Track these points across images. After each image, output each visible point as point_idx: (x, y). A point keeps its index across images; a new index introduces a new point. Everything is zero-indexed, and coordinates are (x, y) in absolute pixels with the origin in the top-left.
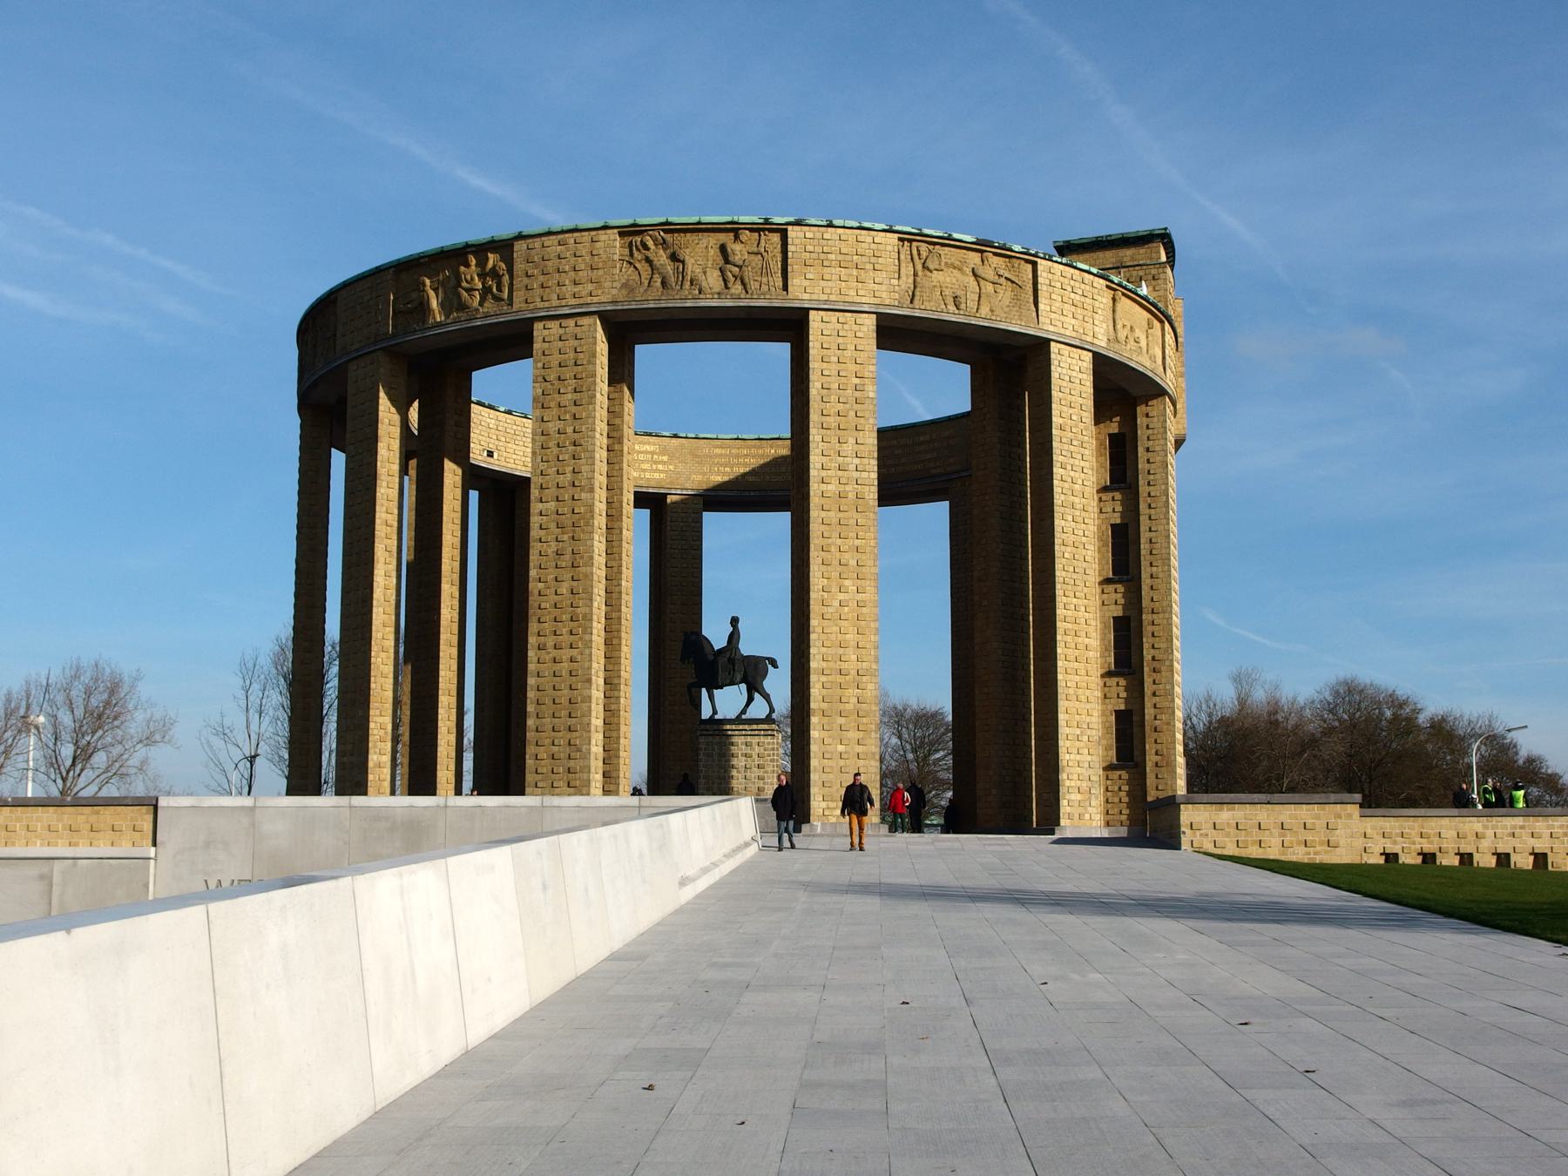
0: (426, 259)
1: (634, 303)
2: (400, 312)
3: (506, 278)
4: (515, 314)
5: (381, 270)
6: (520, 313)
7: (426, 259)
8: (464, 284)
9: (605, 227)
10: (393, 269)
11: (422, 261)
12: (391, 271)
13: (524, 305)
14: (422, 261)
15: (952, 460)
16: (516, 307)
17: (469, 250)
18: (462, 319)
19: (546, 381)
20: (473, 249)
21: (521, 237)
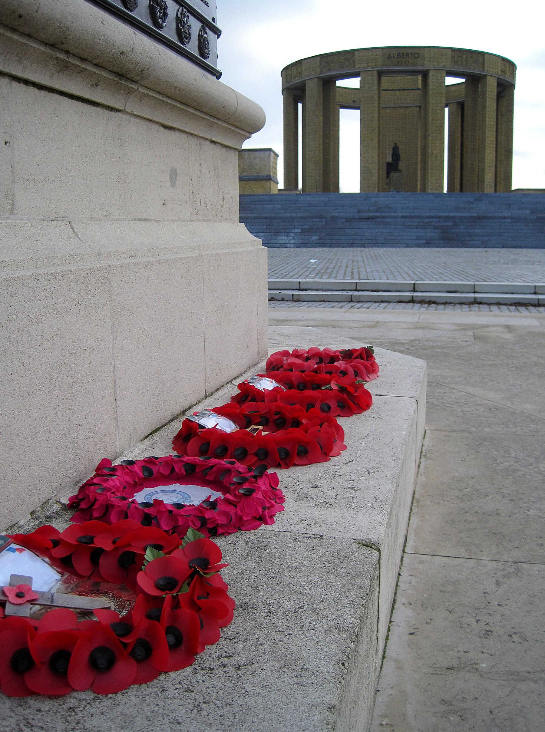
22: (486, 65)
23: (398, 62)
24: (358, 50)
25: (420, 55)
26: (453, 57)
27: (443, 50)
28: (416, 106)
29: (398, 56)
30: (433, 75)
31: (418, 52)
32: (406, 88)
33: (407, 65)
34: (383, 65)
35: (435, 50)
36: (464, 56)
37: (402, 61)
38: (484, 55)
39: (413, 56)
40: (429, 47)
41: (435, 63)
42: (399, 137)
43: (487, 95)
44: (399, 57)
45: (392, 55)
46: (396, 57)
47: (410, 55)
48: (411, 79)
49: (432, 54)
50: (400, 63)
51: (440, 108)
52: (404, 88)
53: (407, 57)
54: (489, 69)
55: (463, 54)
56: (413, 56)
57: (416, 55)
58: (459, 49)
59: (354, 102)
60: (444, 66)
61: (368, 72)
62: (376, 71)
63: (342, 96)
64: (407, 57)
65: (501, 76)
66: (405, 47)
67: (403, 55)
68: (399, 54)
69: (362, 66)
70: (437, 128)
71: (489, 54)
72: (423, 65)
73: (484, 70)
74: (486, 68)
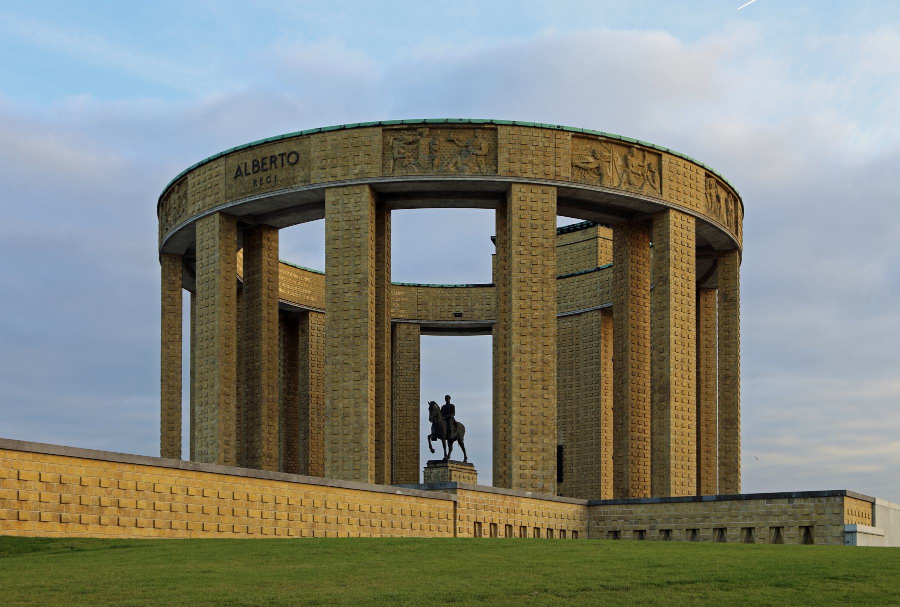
0: (604, 139)
1: (710, 219)
2: (577, 166)
3: (657, 175)
4: (663, 201)
5: (562, 130)
6: (665, 202)
7: (604, 139)
8: (631, 167)
9: (702, 167)
10: (573, 134)
11: (600, 138)
12: (570, 134)
13: (668, 199)
14: (600, 138)
15: (403, 311)
16: (664, 197)
17: (636, 146)
18: (633, 191)
19: (676, 251)
20: (639, 147)
21: (667, 152)
22: (503, 156)
23: (255, 182)
24: (190, 171)
25: (301, 156)
26: (386, 148)
27: (355, 133)
28: (596, 310)
29: (254, 166)
30: (335, 203)
31: (295, 149)
32: (575, 272)
33: (273, 187)
34: (226, 198)
35: (334, 136)
36: (424, 142)
37: (261, 180)
38: (496, 130)
39: (285, 159)
40: (320, 131)
41: (339, 171)
42: (565, 387)
43: (515, 239)
44: (256, 169)
45: (243, 169)
46: (250, 170)
47: (279, 162)
48: (584, 249)
49: (330, 147)
50: (258, 184)
51: (353, 286)
52: (570, 273)
53: (273, 165)
54: (516, 166)
55: (421, 134)
56: (285, 159)
57: (293, 159)
58: (402, 124)
59: (458, 315)
60: (362, 175)
61: (206, 221)
62: (218, 214)
63: (426, 304)
64: (273, 165)
65: (576, 182)
66: (267, 143)
67: (264, 164)
68: (255, 164)
69: (196, 208)
70: (346, 341)
71: (514, 125)
72: (307, 181)
73: (496, 171)
74: (503, 166)
